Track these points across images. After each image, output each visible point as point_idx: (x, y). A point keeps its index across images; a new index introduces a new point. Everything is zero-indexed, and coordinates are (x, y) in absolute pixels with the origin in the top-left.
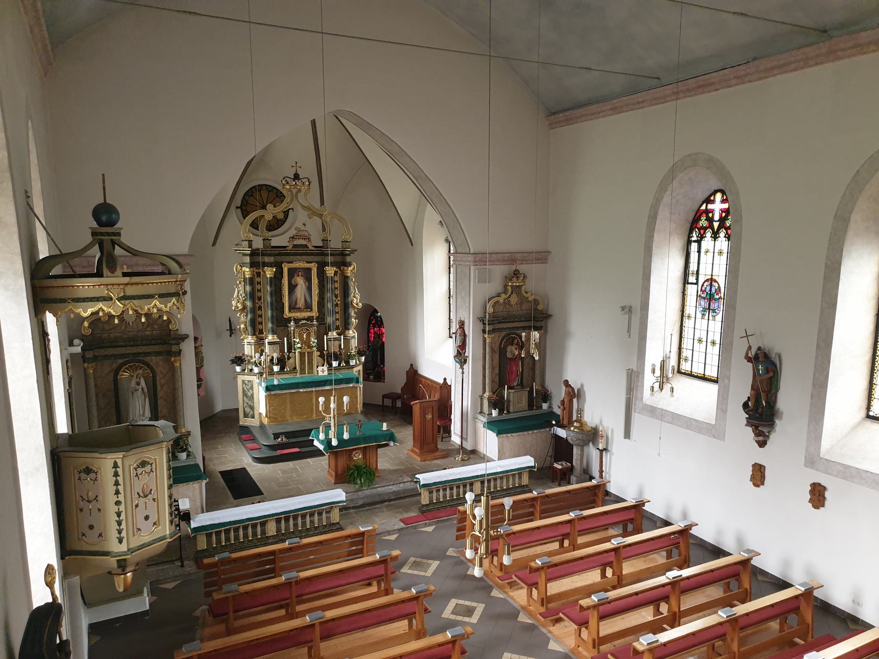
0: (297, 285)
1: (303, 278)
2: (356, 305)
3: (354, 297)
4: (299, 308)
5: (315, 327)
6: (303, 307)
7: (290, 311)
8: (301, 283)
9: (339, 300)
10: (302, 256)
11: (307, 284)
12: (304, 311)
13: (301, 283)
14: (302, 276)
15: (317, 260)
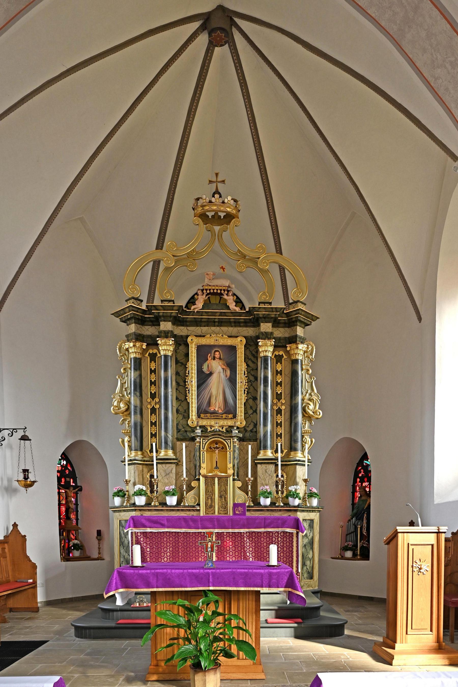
0: (211, 374)
1: (221, 362)
2: (312, 414)
3: (310, 400)
4: (214, 413)
5: (236, 440)
6: (220, 411)
7: (199, 416)
8: (218, 371)
9: (282, 404)
10: (222, 328)
11: (228, 372)
12: (222, 418)
13: (218, 371)
14: (220, 359)
15: (247, 334)
